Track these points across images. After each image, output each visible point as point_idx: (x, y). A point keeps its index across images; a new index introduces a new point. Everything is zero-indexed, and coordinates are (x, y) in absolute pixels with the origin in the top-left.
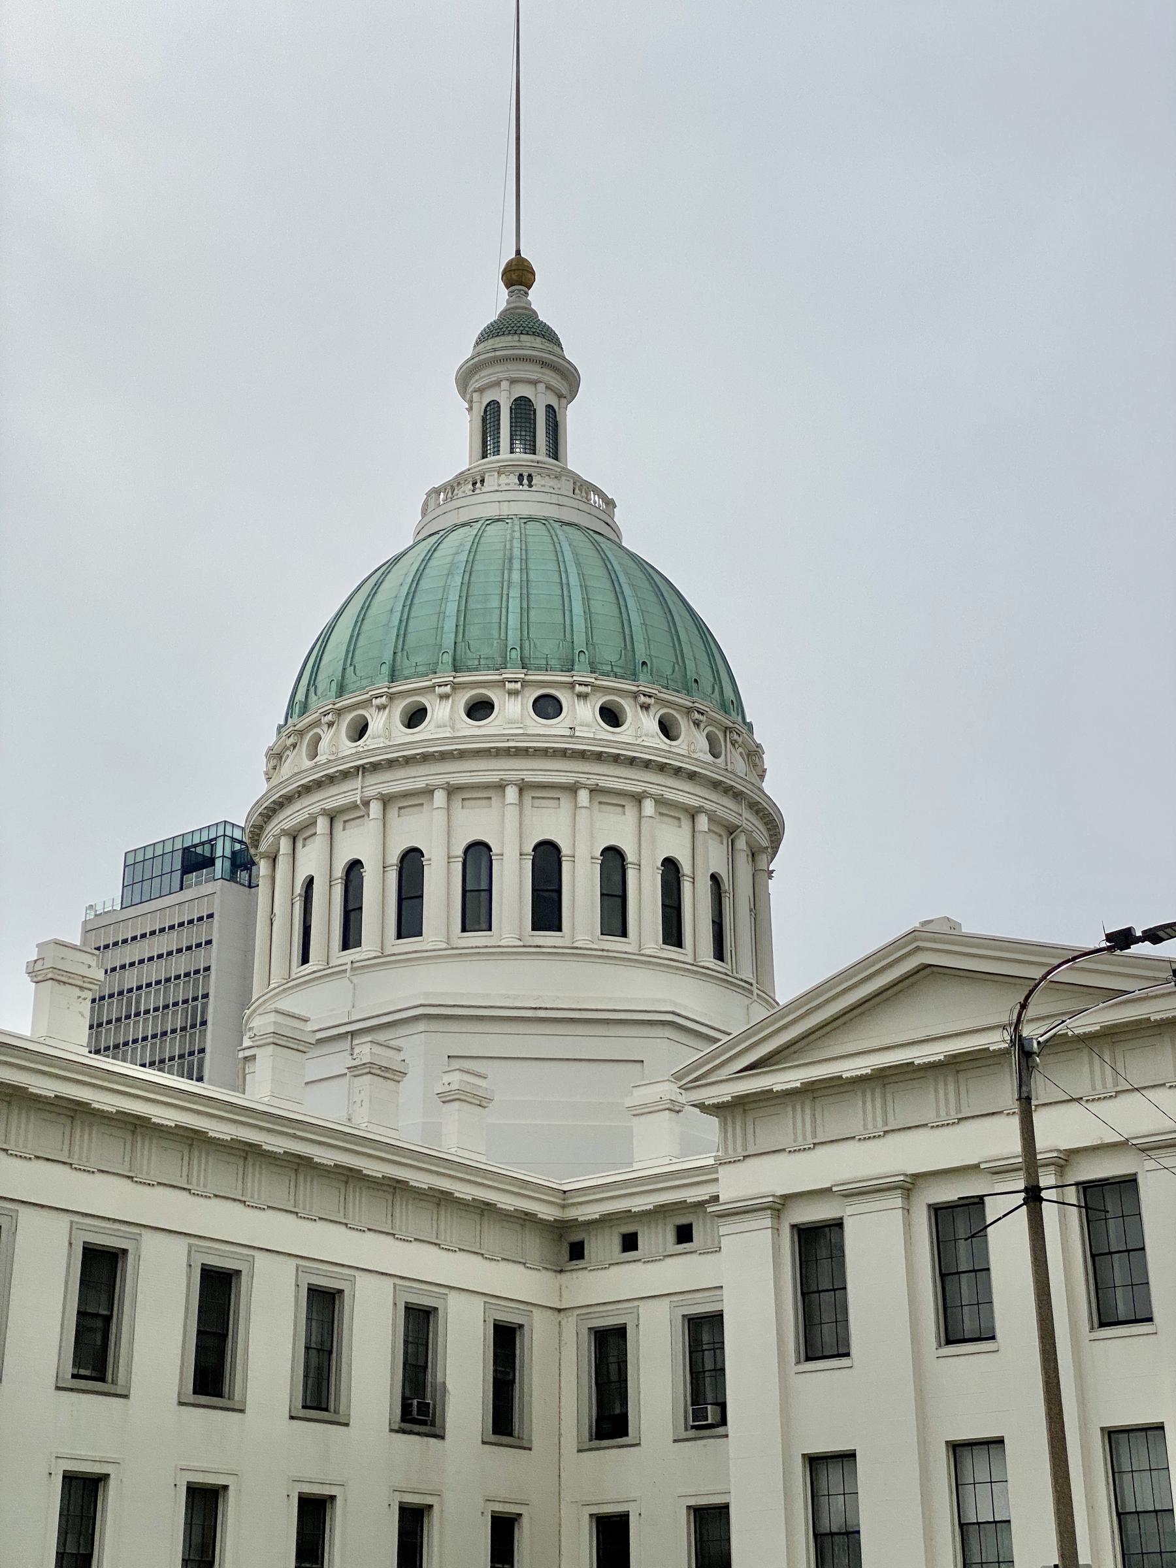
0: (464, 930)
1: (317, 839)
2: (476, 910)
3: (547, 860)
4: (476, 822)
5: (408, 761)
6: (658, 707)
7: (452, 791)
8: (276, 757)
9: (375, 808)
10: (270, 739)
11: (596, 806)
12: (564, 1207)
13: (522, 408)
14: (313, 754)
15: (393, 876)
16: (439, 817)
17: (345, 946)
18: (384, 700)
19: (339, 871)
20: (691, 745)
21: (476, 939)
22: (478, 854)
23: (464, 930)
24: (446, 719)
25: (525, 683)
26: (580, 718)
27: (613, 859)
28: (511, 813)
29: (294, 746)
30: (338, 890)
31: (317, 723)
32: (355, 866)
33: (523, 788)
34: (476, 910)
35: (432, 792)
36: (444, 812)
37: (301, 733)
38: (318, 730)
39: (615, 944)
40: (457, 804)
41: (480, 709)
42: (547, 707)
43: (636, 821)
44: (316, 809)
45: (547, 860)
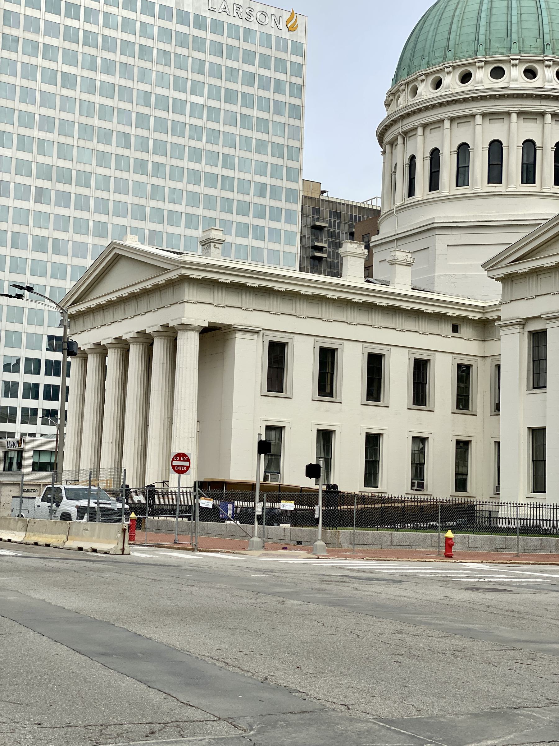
0: (457, 186)
1: (398, 146)
2: (462, 176)
3: (496, 149)
5: (434, 106)
6: (555, 66)
7: (452, 120)
8: (388, 105)
9: (420, 131)
11: (521, 121)
12: (484, 313)
14: (397, 106)
15: (428, 162)
17: (409, 196)
18: (423, 77)
19: (407, 161)
21: (463, 190)
22: (463, 150)
23: (457, 186)
24: (452, 84)
25: (486, 63)
26: (515, 77)
27: (529, 146)
29: (392, 100)
30: (407, 169)
31: (398, 90)
32: (413, 158)
33: (484, 115)
34: (462, 176)
35: (443, 121)
36: (449, 130)
37: (394, 94)
38: (399, 93)
39: (528, 188)
40: (455, 124)
42: (497, 73)
43: (541, 126)
44: (397, 132)
45: (496, 149)
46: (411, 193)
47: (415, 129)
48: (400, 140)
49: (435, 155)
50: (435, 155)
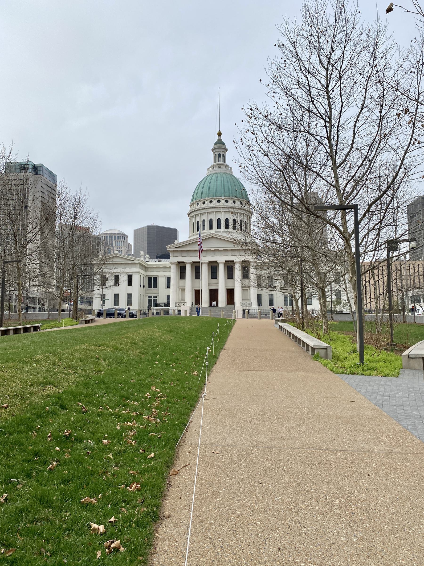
3: (219, 220)
8: (190, 206)
10: (189, 203)
13: (219, 155)
16: (206, 216)
20: (238, 204)
28: (215, 215)
32: (198, 221)
41: (211, 202)
42: (219, 201)
45: (219, 220)
47: (198, 214)
48: (194, 216)
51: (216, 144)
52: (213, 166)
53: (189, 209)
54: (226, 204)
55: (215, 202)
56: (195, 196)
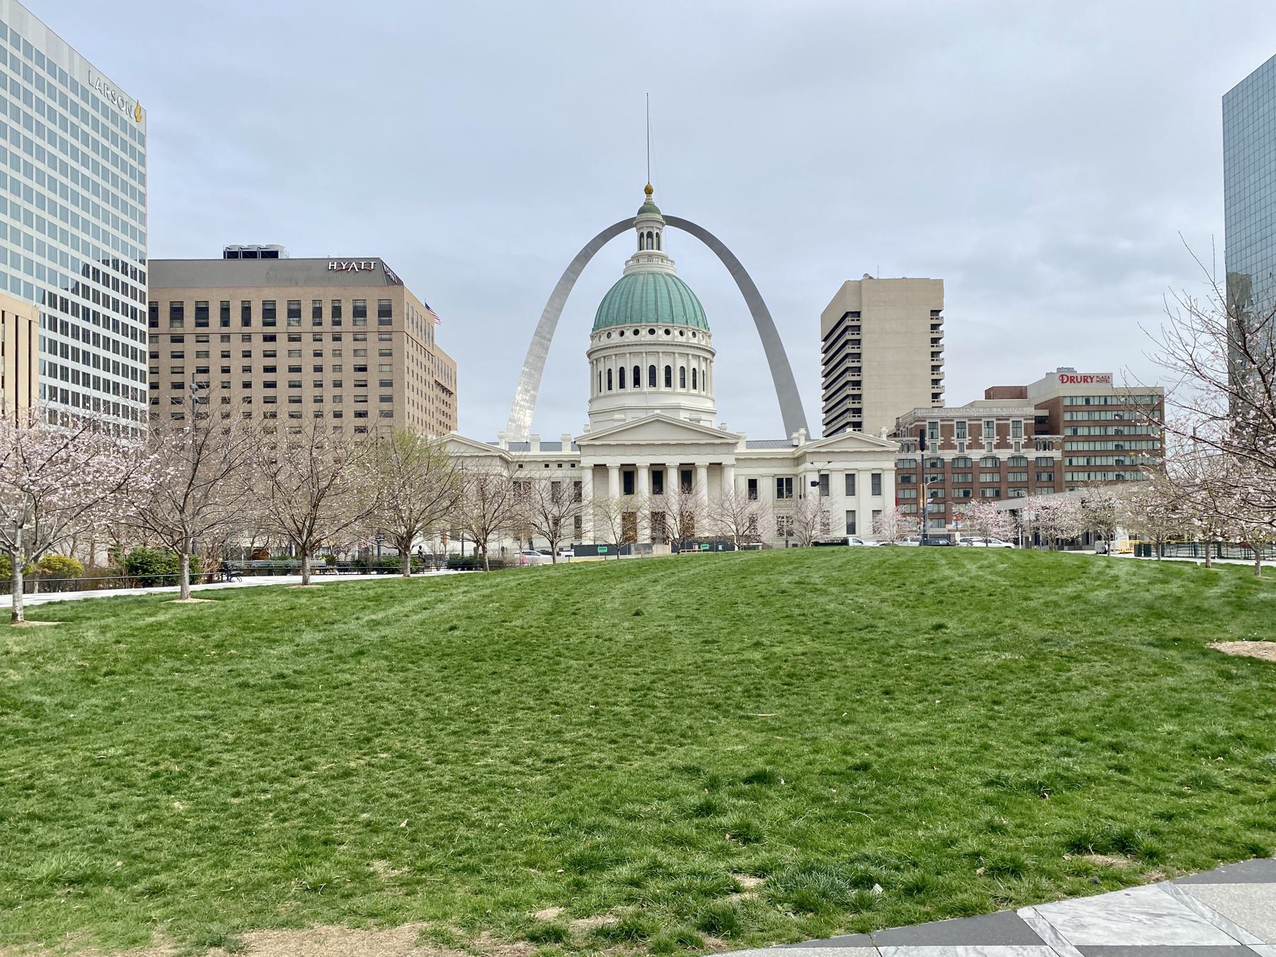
2: (637, 382)
3: (652, 370)
4: (636, 362)
8: (592, 337)
21: (637, 390)
27: (668, 369)
34: (637, 382)
39: (668, 389)
41: (636, 332)
42: (652, 332)
45: (652, 370)
46: (610, 388)
49: (622, 370)
50: (622, 370)
51: (641, 211)
52: (636, 258)
53: (587, 344)
54: (666, 338)
55: (644, 333)
56: (603, 318)
